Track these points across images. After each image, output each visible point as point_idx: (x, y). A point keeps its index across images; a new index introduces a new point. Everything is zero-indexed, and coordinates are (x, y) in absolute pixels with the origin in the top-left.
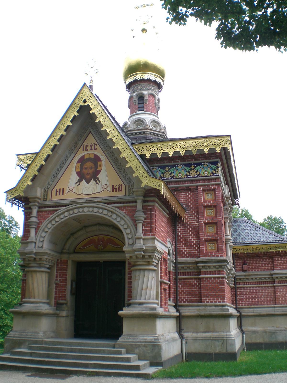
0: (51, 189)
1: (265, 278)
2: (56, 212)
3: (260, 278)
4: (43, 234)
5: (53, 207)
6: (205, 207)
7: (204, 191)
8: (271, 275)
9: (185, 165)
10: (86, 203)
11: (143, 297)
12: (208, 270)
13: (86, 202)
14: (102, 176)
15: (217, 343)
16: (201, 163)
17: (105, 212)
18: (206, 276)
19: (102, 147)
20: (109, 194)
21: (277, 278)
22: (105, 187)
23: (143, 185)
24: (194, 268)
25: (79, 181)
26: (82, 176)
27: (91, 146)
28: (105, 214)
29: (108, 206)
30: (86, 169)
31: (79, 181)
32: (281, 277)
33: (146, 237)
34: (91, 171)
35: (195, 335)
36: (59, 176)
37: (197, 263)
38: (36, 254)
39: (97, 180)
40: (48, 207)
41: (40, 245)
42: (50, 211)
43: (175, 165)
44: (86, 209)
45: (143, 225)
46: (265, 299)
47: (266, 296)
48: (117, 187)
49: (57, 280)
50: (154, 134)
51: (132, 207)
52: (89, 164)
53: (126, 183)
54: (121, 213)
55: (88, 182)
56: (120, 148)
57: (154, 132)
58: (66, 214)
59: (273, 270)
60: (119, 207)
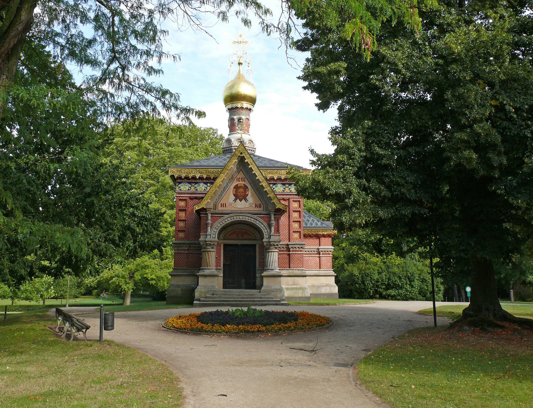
0: (218, 203)
1: (314, 251)
2: (222, 218)
3: (311, 251)
4: (215, 230)
5: (220, 214)
6: (294, 211)
7: (293, 201)
8: (318, 249)
9: (282, 184)
10: (241, 213)
11: (273, 266)
12: (295, 249)
13: (241, 213)
14: (250, 198)
15: (299, 291)
17: (252, 219)
18: (293, 253)
19: (249, 180)
20: (254, 209)
21: (322, 251)
22: (251, 204)
23: (277, 208)
24: (286, 247)
25: (235, 200)
26: (237, 197)
27: (242, 179)
28: (252, 221)
30: (239, 192)
31: (235, 200)
32: (325, 251)
33: (275, 234)
35: (287, 286)
36: (223, 196)
37: (288, 245)
38: (211, 241)
39: (246, 200)
40: (217, 214)
41: (214, 236)
42: (218, 217)
43: (276, 184)
44: (241, 217)
48: (258, 205)
51: (268, 217)
52: (241, 190)
53: (263, 203)
54: (262, 220)
55: (241, 200)
56: (264, 185)
58: (229, 219)
59: (320, 246)
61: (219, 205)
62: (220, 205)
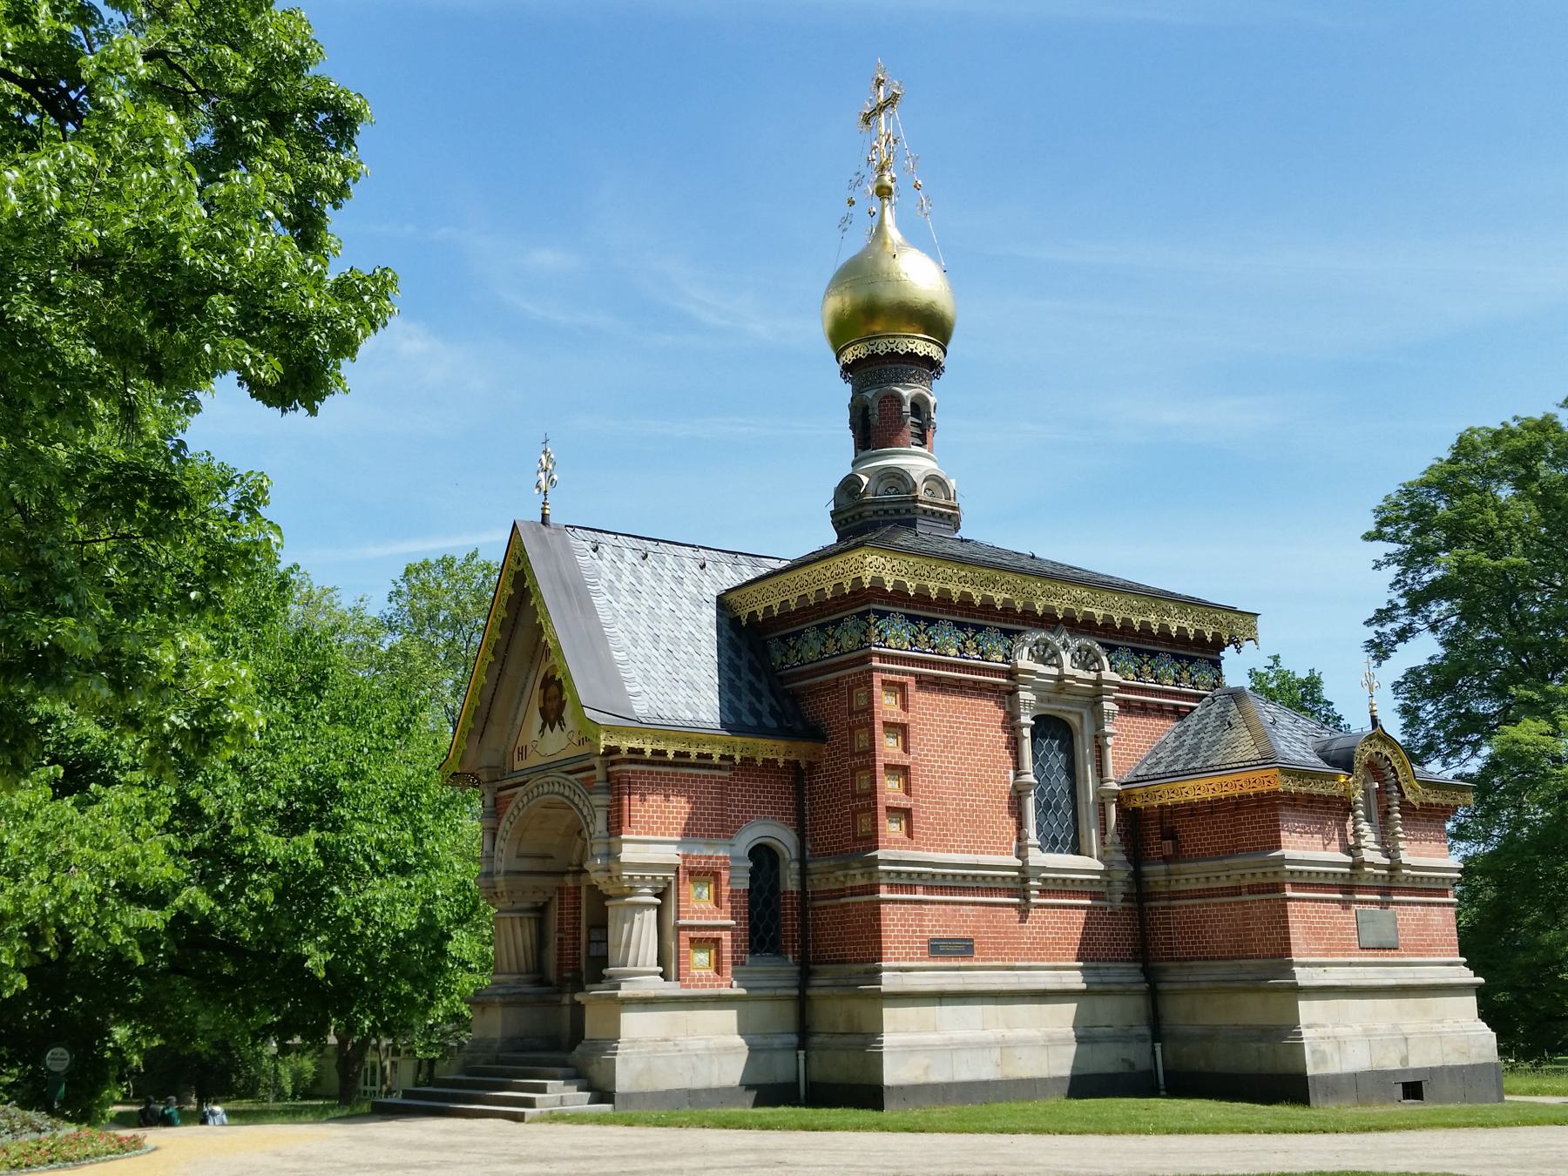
16: (841, 620)
29: (571, 777)
31: (544, 726)
34: (555, 704)
36: (519, 722)
45: (608, 813)
46: (1222, 942)
47: (1227, 931)
49: (561, 930)
50: (886, 512)
52: (553, 690)
57: (885, 507)
60: (583, 779)
61: (516, 754)
62: (516, 754)
